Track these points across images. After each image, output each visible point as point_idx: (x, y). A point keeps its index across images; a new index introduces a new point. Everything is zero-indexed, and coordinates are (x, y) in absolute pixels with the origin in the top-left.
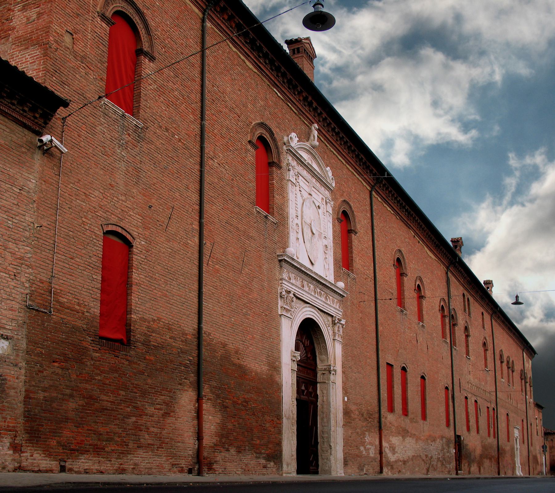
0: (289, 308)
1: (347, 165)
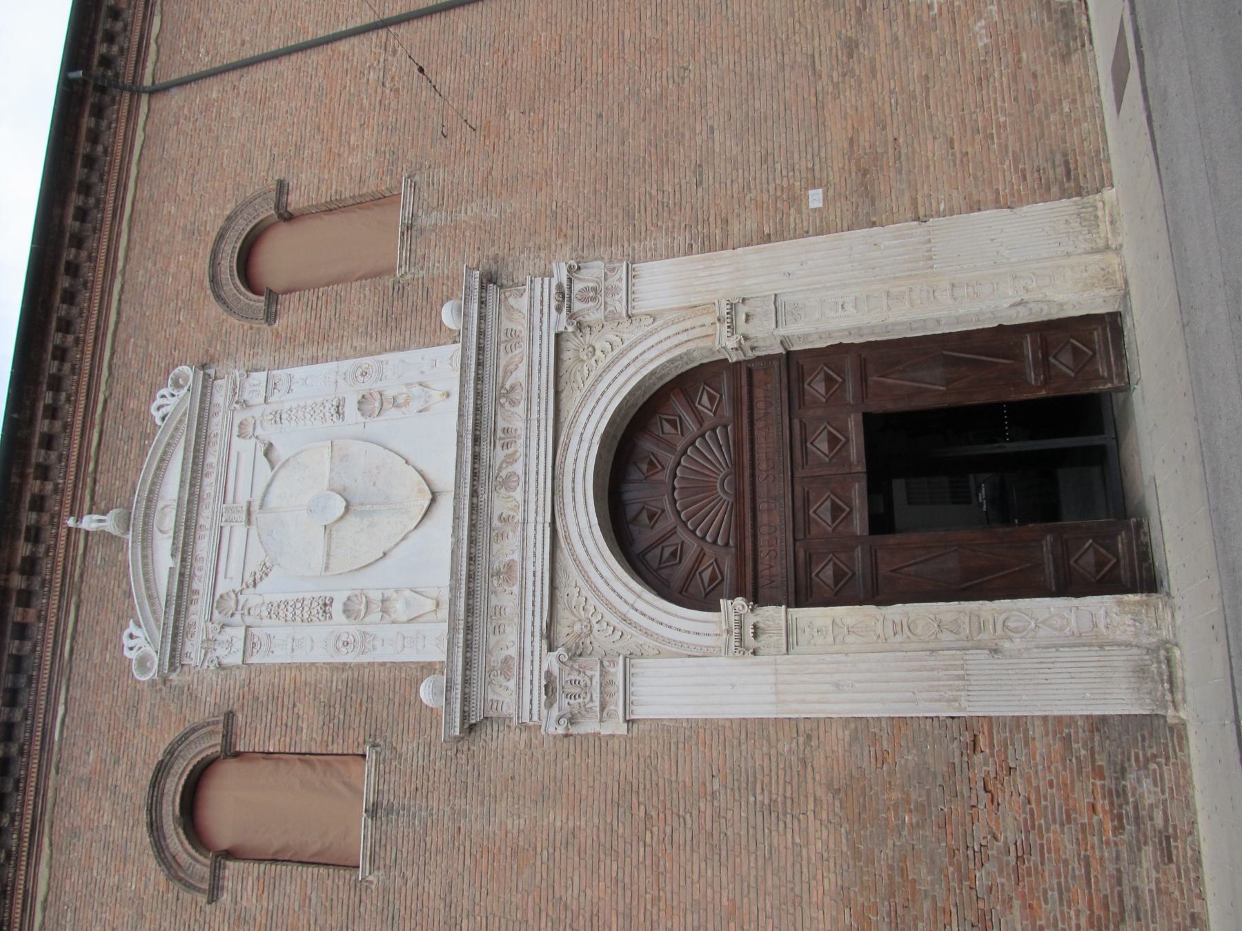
0: (597, 674)
1: (120, 264)
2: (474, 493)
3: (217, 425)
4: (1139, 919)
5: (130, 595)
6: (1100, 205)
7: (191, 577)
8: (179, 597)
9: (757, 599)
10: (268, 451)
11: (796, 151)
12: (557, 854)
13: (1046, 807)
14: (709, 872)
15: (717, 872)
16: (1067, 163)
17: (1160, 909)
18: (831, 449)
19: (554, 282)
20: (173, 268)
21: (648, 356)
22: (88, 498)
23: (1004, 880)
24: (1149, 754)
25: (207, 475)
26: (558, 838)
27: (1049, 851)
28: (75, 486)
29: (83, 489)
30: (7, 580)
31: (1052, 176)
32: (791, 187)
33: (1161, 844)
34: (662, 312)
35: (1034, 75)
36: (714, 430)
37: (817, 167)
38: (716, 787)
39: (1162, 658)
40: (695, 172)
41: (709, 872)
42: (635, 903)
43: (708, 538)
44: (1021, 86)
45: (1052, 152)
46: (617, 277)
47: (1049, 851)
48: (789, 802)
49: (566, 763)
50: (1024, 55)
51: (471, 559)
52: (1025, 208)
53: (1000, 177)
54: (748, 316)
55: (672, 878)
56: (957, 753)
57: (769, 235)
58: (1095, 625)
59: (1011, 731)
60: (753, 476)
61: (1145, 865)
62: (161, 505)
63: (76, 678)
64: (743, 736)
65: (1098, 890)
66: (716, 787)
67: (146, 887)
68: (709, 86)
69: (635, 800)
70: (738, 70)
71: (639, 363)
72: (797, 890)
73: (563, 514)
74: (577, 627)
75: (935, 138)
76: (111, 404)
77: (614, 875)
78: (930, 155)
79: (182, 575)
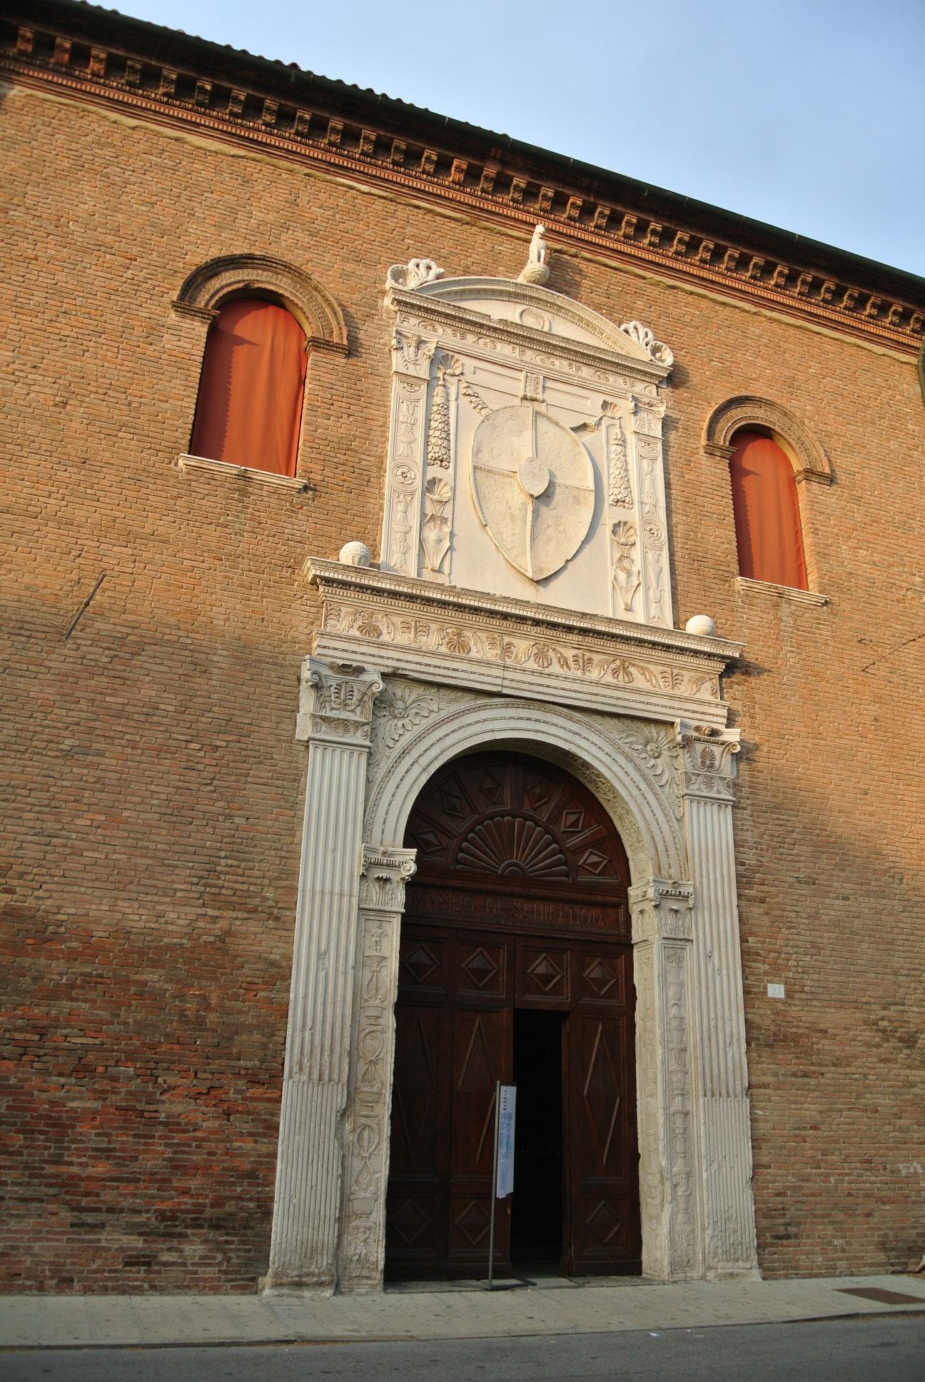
0: (357, 718)
1: (768, 313)
2: (537, 622)
3: (616, 381)
4: (73, 1225)
5: (465, 272)
6: (748, 1265)
7: (480, 335)
8: (461, 320)
9: (412, 886)
11: (820, 977)
12: (187, 653)
13: (190, 1146)
14: (156, 802)
15: (158, 810)
16: (788, 1237)
17: (80, 1248)
18: (538, 976)
19: (722, 728)
20: (760, 362)
21: (646, 809)
23: (123, 1095)
24: (231, 1255)
25: (570, 365)
26: (202, 656)
27: (145, 1144)
28: (571, 237)
30: (494, 159)
31: (779, 1221)
32: (788, 968)
33: (143, 1256)
34: (681, 828)
35: (869, 1215)
36: (565, 864)
37: (803, 996)
38: (237, 820)
39: (324, 1278)
40: (809, 877)
41: (156, 802)
42: (132, 723)
43: (465, 844)
44: (860, 1200)
45: (800, 1223)
46: (722, 790)
47: (145, 1144)
48: (216, 890)
49: (274, 674)
50: (888, 1207)
51: (476, 610)
52: (750, 1192)
53: (781, 1172)
54: (676, 911)
55: (153, 763)
56: (249, 1064)
57: (747, 941)
58: (358, 1216)
59: (265, 1120)
60: (520, 896)
61: (125, 1238)
62: (547, 316)
63: (392, 207)
64: (283, 854)
65: (105, 1187)
66: (237, 820)
67: (191, 243)
68: (885, 901)
69: (232, 738)
70: (896, 930)
72: (131, 887)
73: (507, 706)
74: (400, 704)
75: (821, 1112)
76: (640, 283)
77: (162, 706)
78: (807, 1106)
79: (482, 326)
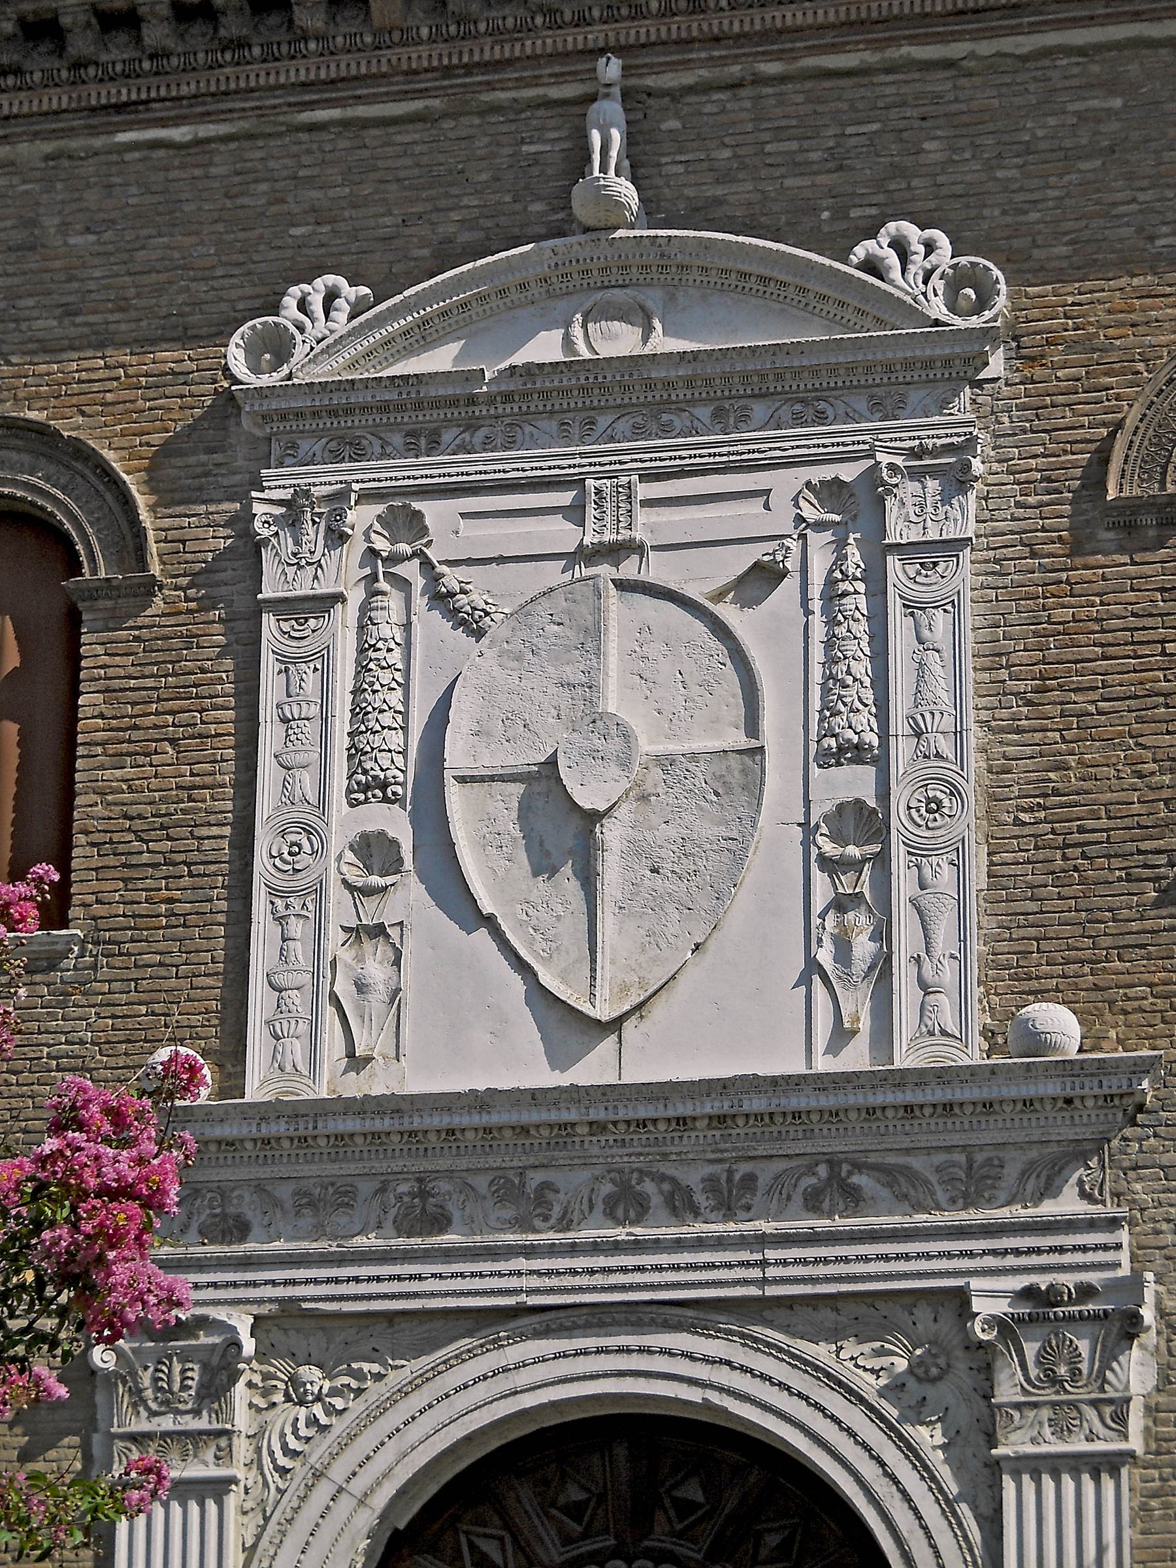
7: (471, 426)
10: (765, 576)
22: (688, 78)
29: (711, 62)
46: (1098, 1427)
71: (882, 1488)
